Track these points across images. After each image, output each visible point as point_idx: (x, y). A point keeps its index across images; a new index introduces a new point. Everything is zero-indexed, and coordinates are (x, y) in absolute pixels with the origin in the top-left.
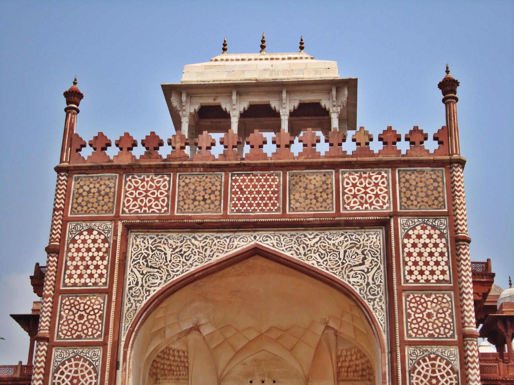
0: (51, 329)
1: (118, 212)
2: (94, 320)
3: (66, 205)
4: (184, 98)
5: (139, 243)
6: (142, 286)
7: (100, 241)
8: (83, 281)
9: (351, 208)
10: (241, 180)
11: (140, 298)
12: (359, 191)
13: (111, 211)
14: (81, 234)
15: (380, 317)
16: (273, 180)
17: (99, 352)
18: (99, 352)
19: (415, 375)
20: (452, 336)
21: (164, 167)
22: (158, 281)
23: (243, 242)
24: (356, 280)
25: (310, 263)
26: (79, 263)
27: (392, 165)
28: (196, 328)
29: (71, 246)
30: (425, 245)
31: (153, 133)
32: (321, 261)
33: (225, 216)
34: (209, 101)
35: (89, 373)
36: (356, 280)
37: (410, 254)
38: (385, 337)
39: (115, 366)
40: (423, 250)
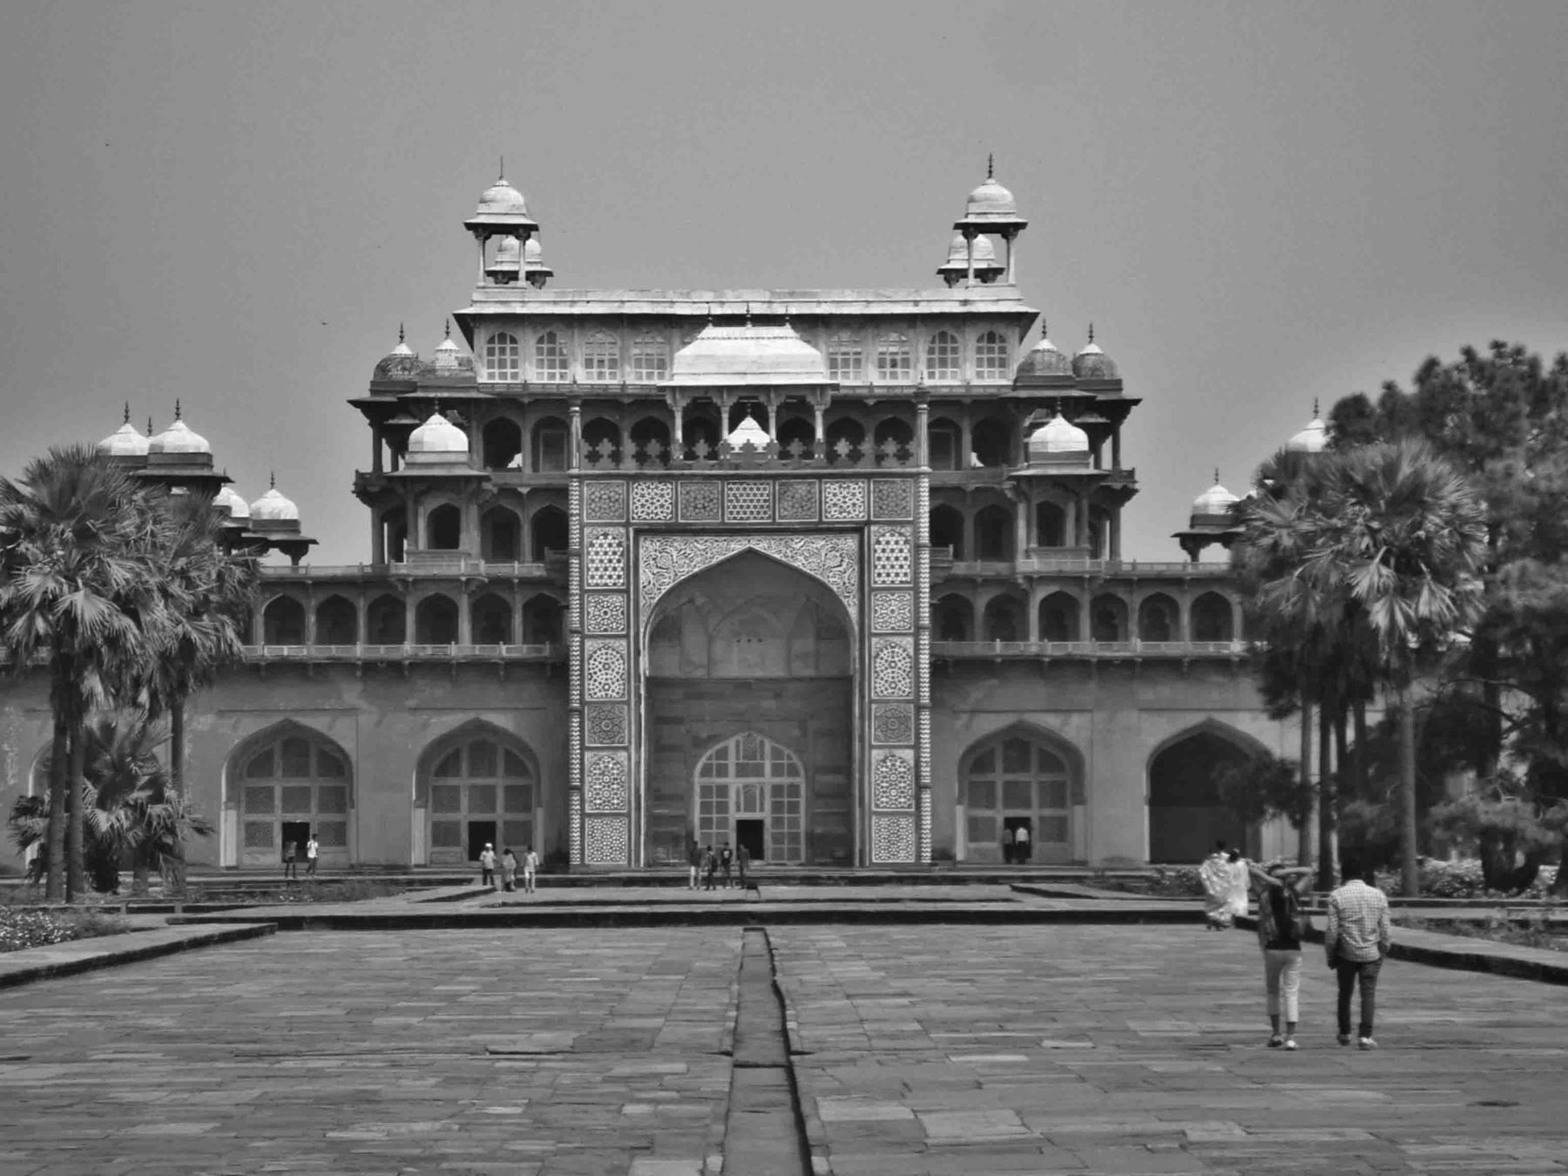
0: (582, 622)
3: (581, 510)
4: (678, 396)
5: (649, 547)
10: (733, 490)
13: (621, 517)
15: (853, 612)
17: (624, 643)
18: (624, 643)
21: (668, 476)
23: (737, 546)
25: (796, 564)
28: (691, 601)
33: (723, 523)
34: (701, 394)
37: (879, 559)
38: (856, 628)
39: (638, 653)
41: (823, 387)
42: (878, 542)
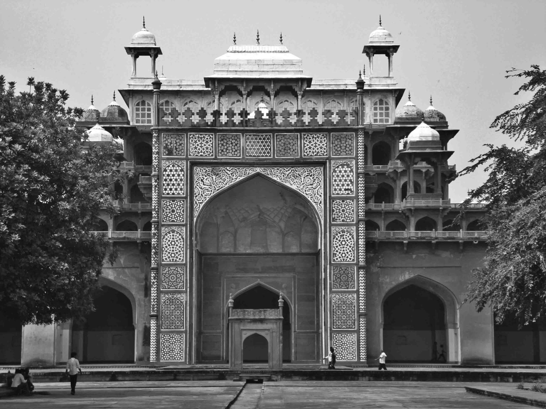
1: (187, 155)
2: (180, 213)
6: (202, 195)
7: (179, 171)
8: (172, 192)
9: (308, 154)
11: (201, 201)
12: (312, 145)
14: (169, 166)
16: (268, 139)
18: (184, 229)
19: (335, 240)
20: (353, 221)
22: (210, 193)
23: (251, 172)
24: (309, 192)
26: (170, 182)
27: (329, 131)
29: (164, 173)
30: (343, 176)
31: (202, 109)
32: (292, 183)
35: (180, 239)
36: (309, 192)
37: (335, 181)
40: (342, 178)
41: (302, 80)
42: (335, 171)
